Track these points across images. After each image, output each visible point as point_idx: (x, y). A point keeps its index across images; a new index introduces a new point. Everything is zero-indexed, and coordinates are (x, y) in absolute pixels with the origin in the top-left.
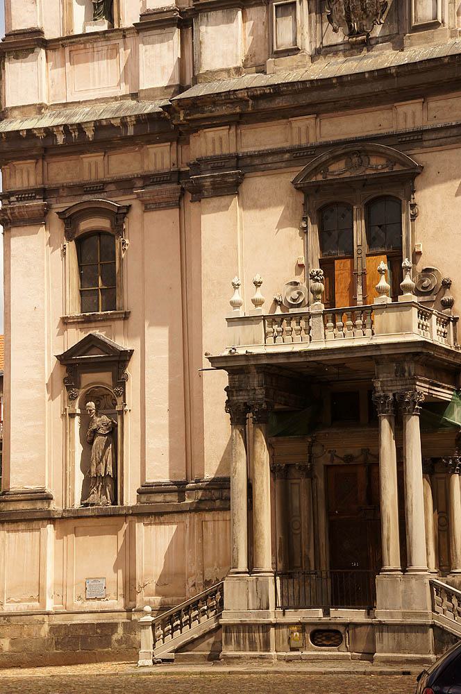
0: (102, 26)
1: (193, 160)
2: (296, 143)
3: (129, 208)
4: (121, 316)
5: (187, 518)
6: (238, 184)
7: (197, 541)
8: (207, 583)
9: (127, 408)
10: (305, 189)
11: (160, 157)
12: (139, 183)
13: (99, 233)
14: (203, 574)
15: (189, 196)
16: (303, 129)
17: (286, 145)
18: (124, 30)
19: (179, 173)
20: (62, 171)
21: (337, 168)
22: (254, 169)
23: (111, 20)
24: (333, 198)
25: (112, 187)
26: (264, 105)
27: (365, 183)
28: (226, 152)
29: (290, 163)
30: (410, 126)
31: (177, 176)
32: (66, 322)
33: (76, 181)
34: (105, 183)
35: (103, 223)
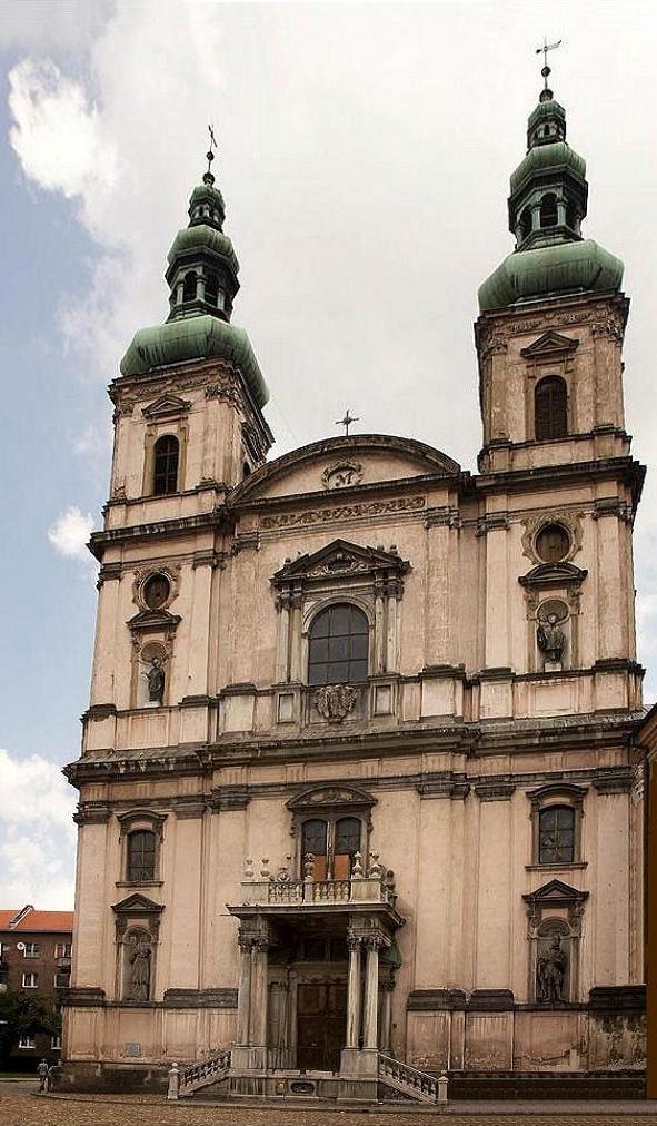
0: (155, 704)
1: (215, 787)
2: (289, 780)
3: (166, 816)
5: (199, 1012)
6: (247, 803)
10: (293, 808)
11: (191, 786)
13: (145, 832)
16: (295, 772)
17: (283, 781)
19: (203, 796)
20: (121, 792)
21: (317, 798)
22: (258, 794)
24: (312, 817)
25: (155, 802)
26: (269, 753)
27: (336, 808)
28: (239, 783)
33: (131, 797)
34: (152, 800)
35: (148, 825)
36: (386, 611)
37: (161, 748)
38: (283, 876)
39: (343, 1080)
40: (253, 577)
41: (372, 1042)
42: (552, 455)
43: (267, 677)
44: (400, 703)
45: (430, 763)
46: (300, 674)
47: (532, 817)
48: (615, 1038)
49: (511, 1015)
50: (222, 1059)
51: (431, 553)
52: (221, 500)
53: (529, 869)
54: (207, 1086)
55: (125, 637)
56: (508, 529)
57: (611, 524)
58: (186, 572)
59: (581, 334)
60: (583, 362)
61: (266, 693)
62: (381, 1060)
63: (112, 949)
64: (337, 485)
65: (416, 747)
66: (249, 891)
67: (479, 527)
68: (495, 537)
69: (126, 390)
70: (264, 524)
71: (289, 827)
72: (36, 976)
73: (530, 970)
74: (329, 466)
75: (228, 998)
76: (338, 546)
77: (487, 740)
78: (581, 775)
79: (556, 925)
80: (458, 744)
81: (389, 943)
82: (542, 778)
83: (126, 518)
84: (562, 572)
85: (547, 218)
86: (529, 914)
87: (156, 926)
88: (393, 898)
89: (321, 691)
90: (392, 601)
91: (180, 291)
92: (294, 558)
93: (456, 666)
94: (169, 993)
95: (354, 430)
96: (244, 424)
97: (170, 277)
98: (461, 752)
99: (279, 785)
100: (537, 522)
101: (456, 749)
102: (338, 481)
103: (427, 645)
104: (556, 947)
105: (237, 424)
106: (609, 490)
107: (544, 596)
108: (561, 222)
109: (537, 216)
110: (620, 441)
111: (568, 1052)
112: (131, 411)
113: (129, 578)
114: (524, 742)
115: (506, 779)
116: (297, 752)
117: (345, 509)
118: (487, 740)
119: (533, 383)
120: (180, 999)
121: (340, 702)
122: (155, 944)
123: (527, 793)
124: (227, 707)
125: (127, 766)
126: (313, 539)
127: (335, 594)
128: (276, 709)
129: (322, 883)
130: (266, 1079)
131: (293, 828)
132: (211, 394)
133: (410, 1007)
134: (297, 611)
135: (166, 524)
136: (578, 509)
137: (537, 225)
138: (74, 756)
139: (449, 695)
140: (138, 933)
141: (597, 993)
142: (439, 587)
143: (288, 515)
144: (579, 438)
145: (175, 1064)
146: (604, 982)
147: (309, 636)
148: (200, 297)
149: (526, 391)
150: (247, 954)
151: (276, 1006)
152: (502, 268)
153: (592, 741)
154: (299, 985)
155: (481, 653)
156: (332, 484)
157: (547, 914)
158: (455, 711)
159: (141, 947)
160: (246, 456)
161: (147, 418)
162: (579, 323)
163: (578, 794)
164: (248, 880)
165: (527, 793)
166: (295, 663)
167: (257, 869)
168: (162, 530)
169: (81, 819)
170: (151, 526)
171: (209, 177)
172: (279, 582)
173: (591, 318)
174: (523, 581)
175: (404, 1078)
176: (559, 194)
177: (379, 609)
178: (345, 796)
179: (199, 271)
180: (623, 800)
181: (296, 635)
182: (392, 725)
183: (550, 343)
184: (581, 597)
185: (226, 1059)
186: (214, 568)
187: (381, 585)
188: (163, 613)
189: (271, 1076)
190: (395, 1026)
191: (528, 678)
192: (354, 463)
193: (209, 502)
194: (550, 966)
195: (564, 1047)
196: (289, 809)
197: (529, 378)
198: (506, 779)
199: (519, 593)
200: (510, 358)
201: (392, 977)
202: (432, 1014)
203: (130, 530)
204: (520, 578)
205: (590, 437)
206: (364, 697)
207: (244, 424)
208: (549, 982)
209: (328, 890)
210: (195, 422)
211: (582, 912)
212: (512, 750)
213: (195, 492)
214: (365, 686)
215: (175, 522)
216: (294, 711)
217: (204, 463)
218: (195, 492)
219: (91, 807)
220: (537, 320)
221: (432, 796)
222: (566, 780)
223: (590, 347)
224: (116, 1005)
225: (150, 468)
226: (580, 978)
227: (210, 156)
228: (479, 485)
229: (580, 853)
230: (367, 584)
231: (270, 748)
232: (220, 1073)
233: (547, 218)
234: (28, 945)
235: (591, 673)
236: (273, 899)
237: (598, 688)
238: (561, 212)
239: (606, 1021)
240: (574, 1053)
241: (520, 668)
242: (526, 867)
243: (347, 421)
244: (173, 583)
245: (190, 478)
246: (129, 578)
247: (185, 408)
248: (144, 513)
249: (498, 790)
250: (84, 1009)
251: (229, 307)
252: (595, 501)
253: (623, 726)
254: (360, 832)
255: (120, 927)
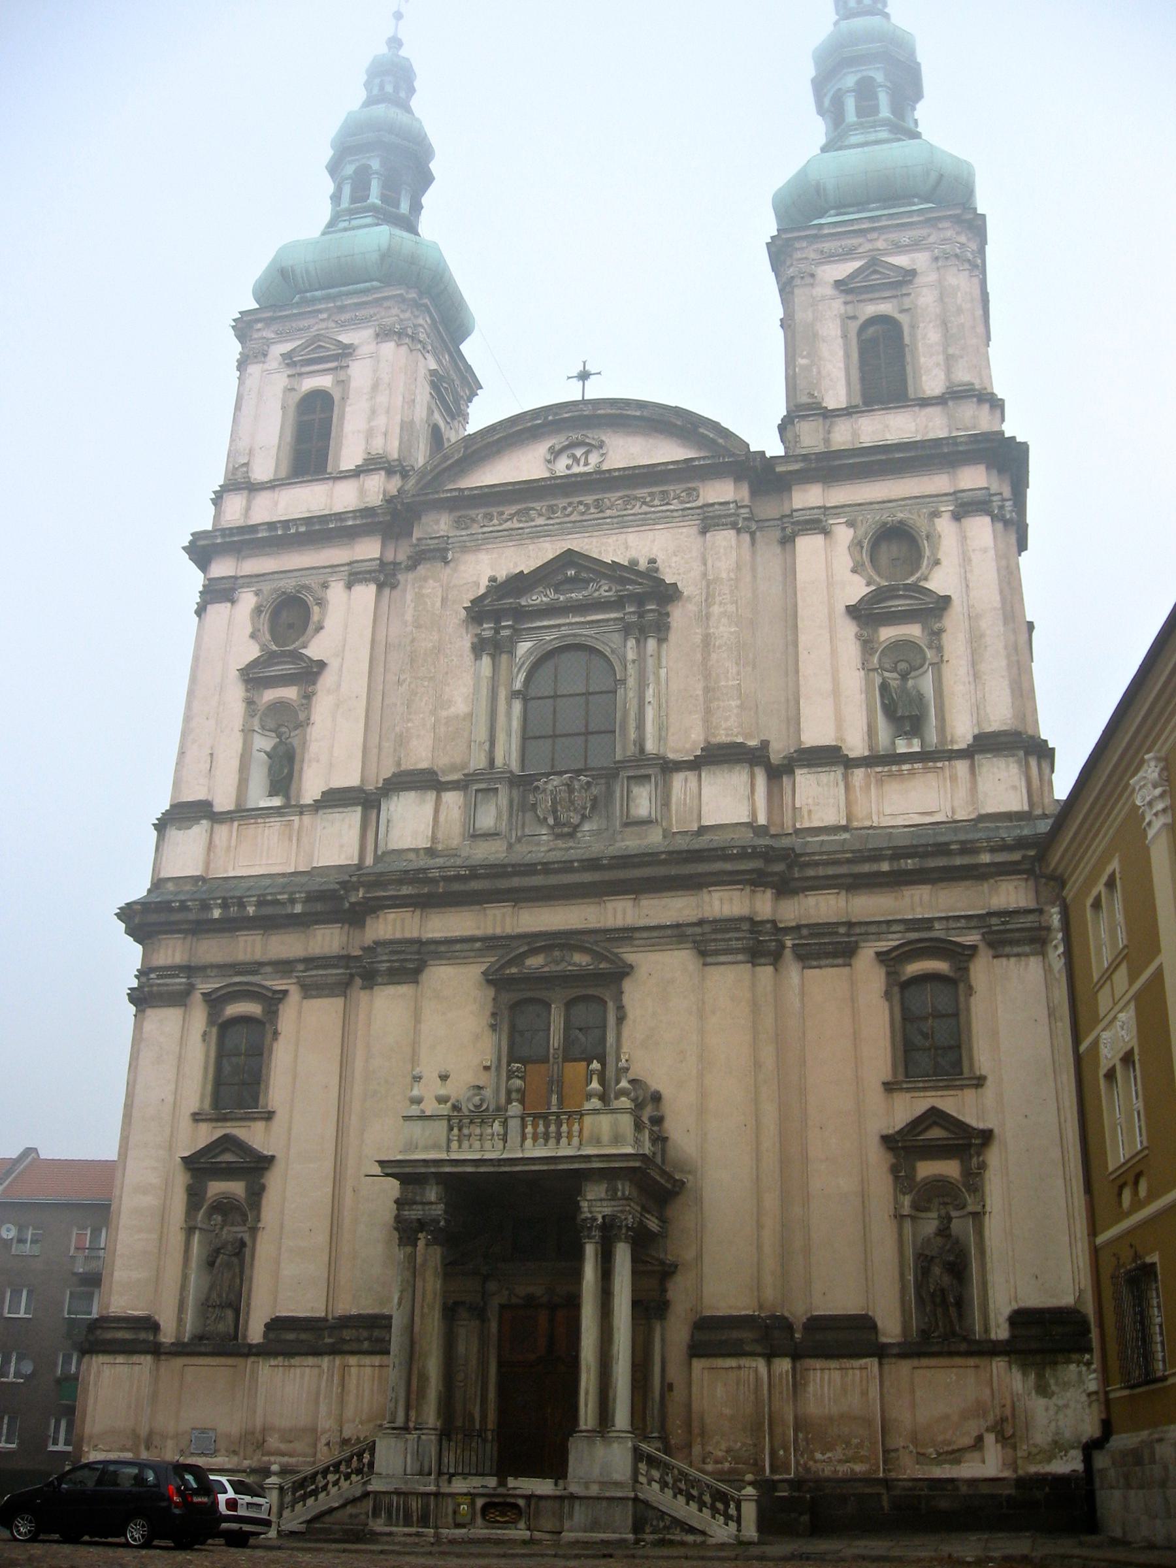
0: (277, 802)
3: (285, 992)
4: (263, 1115)
5: (325, 1361)
7: (336, 1389)
8: (345, 1442)
9: (260, 1225)
10: (495, 980)
12: (301, 967)
14: (341, 1431)
15: (358, 981)
17: (478, 933)
18: (302, 806)
20: (212, 950)
21: (535, 962)
23: (287, 797)
25: (269, 969)
28: (408, 935)
29: (481, 952)
30: (619, 923)
31: (344, 960)
32: (197, 1117)
34: (261, 964)
35: (252, 1008)
36: (641, 660)
37: (283, 875)
38: (477, 1100)
39: (573, 1497)
40: (438, 604)
41: (622, 1417)
42: (887, 426)
43: (458, 760)
44: (666, 803)
45: (717, 903)
46: (508, 754)
47: (888, 995)
48: (1059, 1409)
49: (872, 1363)
50: (360, 1455)
51: (710, 572)
52: (394, 486)
53: (889, 1087)
54: (331, 1511)
55: (236, 693)
56: (826, 532)
57: (981, 529)
58: (336, 593)
59: (919, 260)
60: (925, 298)
61: (454, 786)
62: (638, 1455)
63: (176, 1238)
64: (568, 467)
65: (691, 876)
66: (417, 1130)
67: (784, 529)
68: (808, 546)
69: (259, 326)
70: (459, 524)
71: (488, 1013)
72: (30, 1293)
73: (902, 1275)
74: (558, 441)
75: (376, 1333)
76: (569, 558)
77: (807, 865)
78: (962, 923)
79: (939, 1190)
80: (760, 873)
81: (653, 1224)
82: (900, 928)
83: (248, 509)
84: (911, 597)
85: (867, 107)
86: (894, 1170)
87: (256, 1193)
88: (660, 1140)
89: (540, 784)
90: (651, 644)
91: (347, 190)
92: (502, 575)
93: (753, 743)
94: (276, 1325)
95: (596, 390)
96: (433, 373)
97: (334, 169)
98: (766, 885)
99: (472, 939)
100: (870, 521)
101: (756, 881)
102: (570, 462)
103: (708, 711)
104: (944, 1231)
105: (422, 372)
106: (974, 478)
107: (887, 633)
108: (885, 112)
109: (850, 104)
110: (986, 407)
111: (980, 1439)
112: (265, 355)
113: (247, 600)
114: (866, 868)
115: (842, 930)
116: (504, 884)
117: (580, 503)
118: (807, 865)
119: (854, 326)
120: (291, 1336)
121: (572, 802)
122: (254, 1230)
123: (878, 954)
124: (392, 808)
125: (225, 906)
126: (531, 547)
127: (565, 631)
128: (470, 811)
129: (536, 1117)
130: (437, 1495)
131: (494, 1015)
132: (383, 334)
133: (697, 1350)
134: (504, 657)
135: (308, 521)
136: (930, 504)
137: (851, 116)
138: (138, 889)
139: (744, 790)
140: (225, 1208)
141: (1021, 1318)
142: (724, 620)
143: (494, 510)
144: (925, 402)
145: (275, 1468)
146: (1034, 1299)
147: (523, 695)
148: (374, 198)
149: (845, 336)
150: (409, 1249)
151: (461, 1349)
152: (803, 173)
153: (976, 867)
154: (502, 1307)
155: (794, 722)
156: (562, 466)
157: (926, 1169)
158: (754, 814)
159: (229, 1233)
160: (437, 416)
161: (288, 364)
162: (915, 246)
163: (962, 956)
164: (414, 1110)
165: (878, 954)
166: (501, 737)
167: (430, 1089)
168: (302, 529)
169: (142, 998)
170: (286, 524)
171: (395, 42)
172: (478, 612)
173: (932, 239)
174: (853, 611)
175: (681, 1492)
176: (879, 77)
177: (631, 655)
178: (581, 959)
179: (375, 164)
180: (1034, 964)
181: (502, 694)
182: (654, 839)
183: (875, 272)
184: (944, 636)
185: (367, 1456)
186: (380, 587)
187: (634, 618)
188: (296, 656)
189: (445, 1489)
190: (670, 1387)
191: (871, 761)
192: (592, 436)
193: (376, 488)
194: (937, 1270)
195: (973, 1427)
196: (489, 982)
197: (849, 318)
198: (842, 930)
199: (848, 630)
200: (818, 291)
201: (664, 1290)
202: (731, 1362)
203: (254, 528)
204: (847, 607)
205: (940, 401)
206: (610, 793)
207: (433, 373)
208: (938, 1300)
209: (547, 1126)
210: (359, 373)
211: (983, 1166)
212: (850, 880)
213: (357, 473)
214: (611, 774)
215: (324, 519)
216: (499, 817)
217: (369, 434)
218: (357, 473)
219: (159, 977)
220: (855, 241)
221: (722, 959)
222: (938, 932)
223: (932, 277)
224: (181, 1350)
225: (289, 437)
226: (990, 1292)
227: (398, 16)
228: (779, 469)
229: (971, 1059)
230: (613, 615)
231: (458, 878)
232: (350, 1487)
233: (867, 107)
234: (21, 1228)
235: (967, 754)
236: (455, 1145)
237: (979, 779)
238: (883, 99)
239: (1040, 1376)
240: (990, 1438)
241: (856, 746)
242: (884, 1084)
243: (584, 376)
244: (316, 609)
245: (350, 454)
246: (247, 600)
247: (346, 352)
248: (276, 504)
249: (830, 948)
250: (120, 1359)
251: (416, 207)
252: (955, 493)
253: (1021, 843)
254: (605, 1019)
255: (195, 1195)
